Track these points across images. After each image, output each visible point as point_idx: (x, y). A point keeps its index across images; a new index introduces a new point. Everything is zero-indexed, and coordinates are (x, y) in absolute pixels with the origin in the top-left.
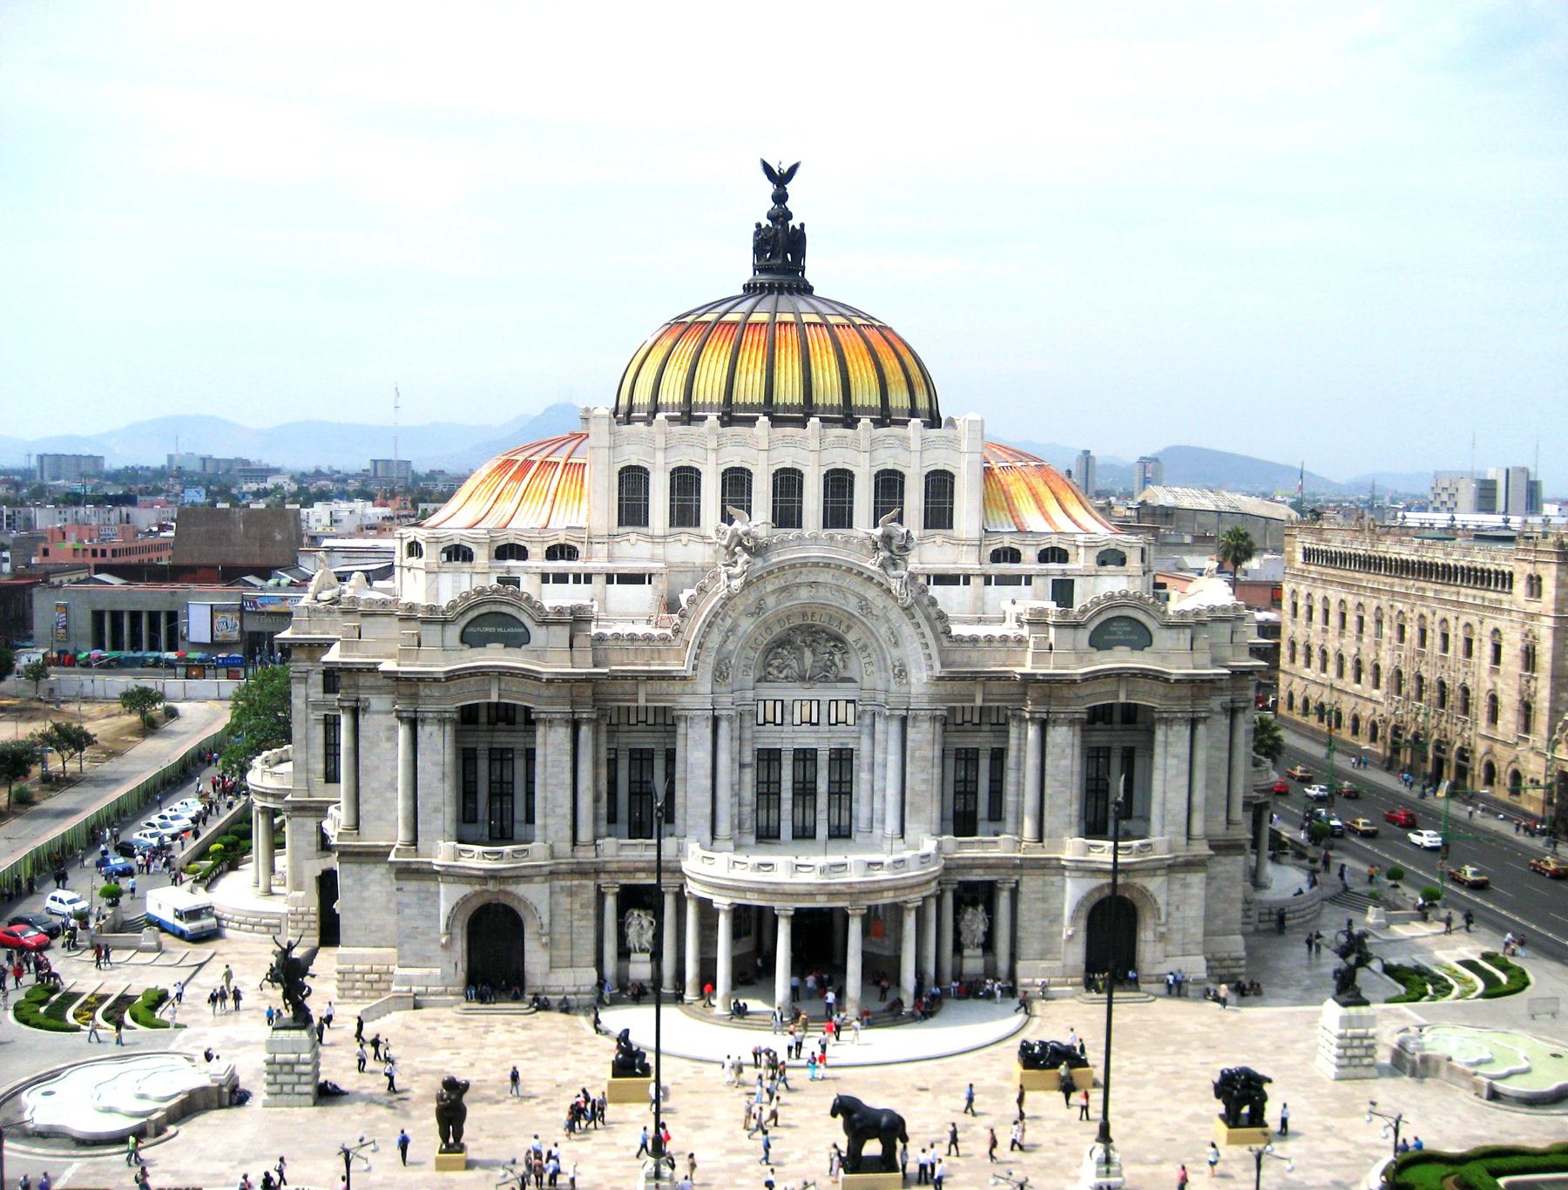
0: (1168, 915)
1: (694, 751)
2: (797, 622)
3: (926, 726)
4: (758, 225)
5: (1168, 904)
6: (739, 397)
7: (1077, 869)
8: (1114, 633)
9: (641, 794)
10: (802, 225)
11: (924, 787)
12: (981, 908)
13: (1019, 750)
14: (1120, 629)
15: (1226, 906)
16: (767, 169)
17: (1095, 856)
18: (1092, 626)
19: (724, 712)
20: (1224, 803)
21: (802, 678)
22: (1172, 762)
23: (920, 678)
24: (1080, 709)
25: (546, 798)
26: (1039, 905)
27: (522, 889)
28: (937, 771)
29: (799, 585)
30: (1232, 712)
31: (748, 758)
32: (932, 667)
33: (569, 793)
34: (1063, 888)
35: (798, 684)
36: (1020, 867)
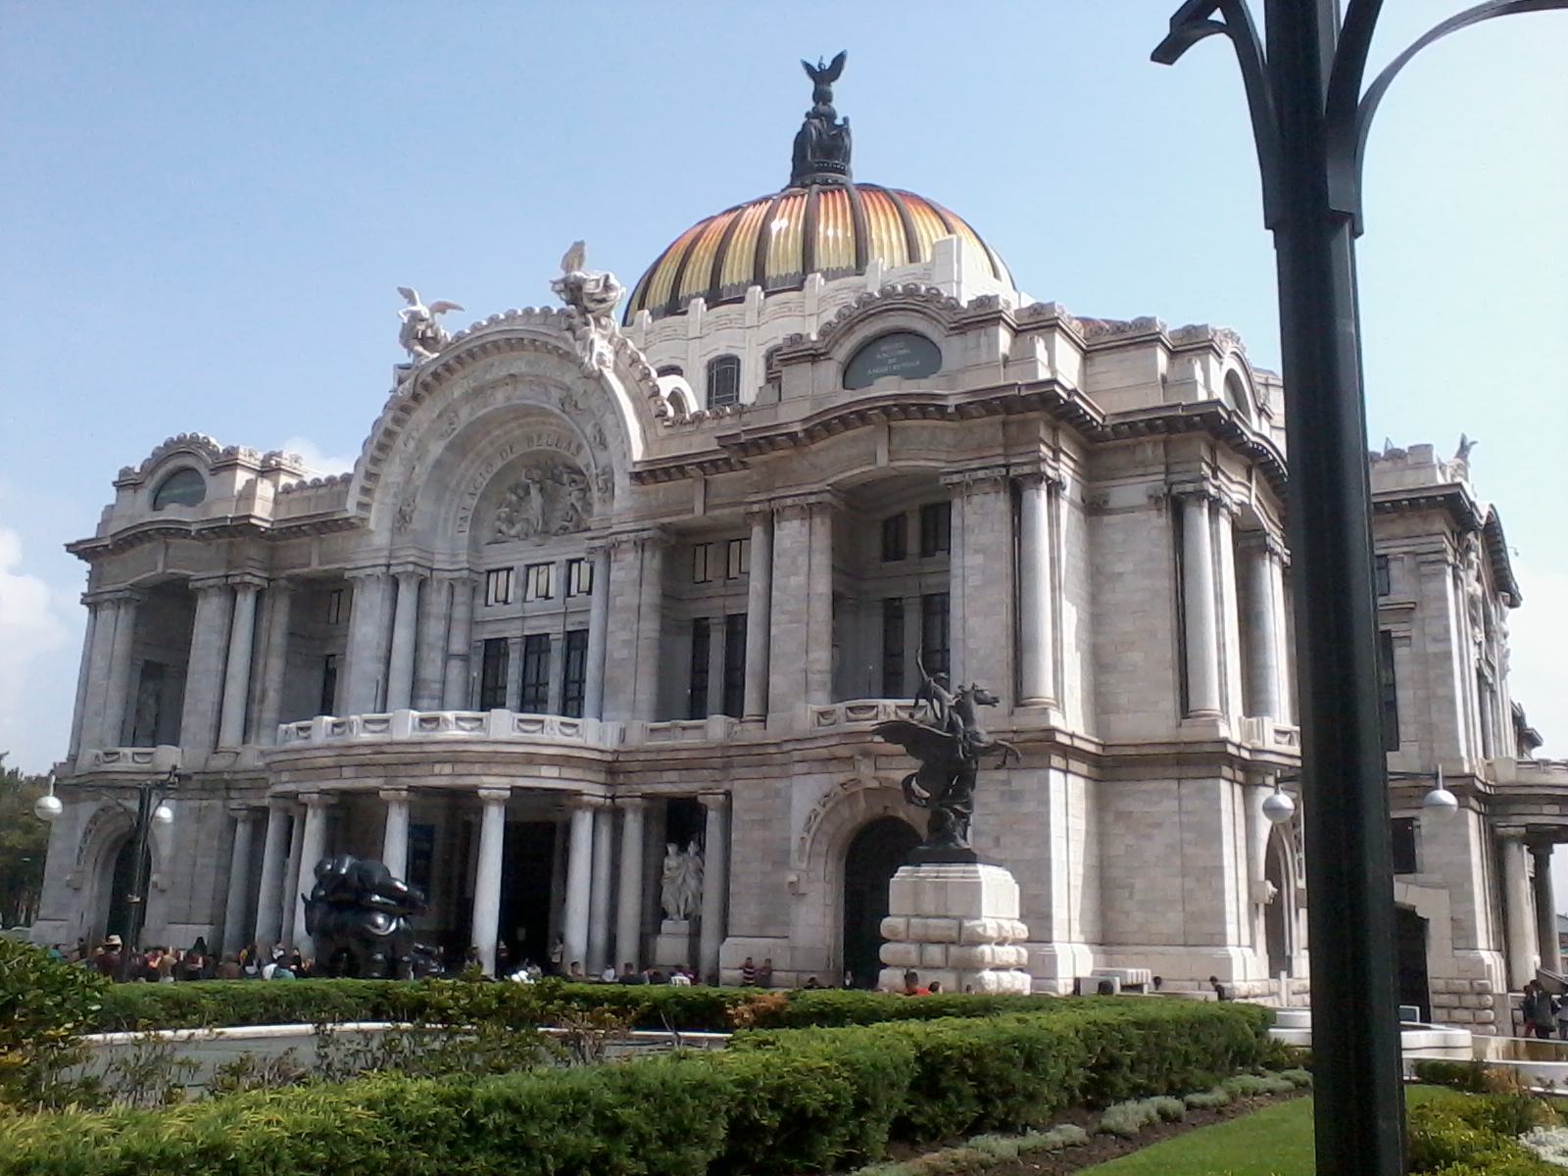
1: (365, 627)
2: (520, 449)
6: (684, 292)
8: (883, 363)
10: (846, 120)
11: (624, 653)
15: (1190, 883)
16: (808, 67)
18: (842, 353)
19: (400, 569)
20: (1170, 676)
22: (974, 560)
23: (622, 482)
26: (757, 834)
29: (495, 385)
30: (1176, 507)
31: (458, 645)
33: (216, 680)
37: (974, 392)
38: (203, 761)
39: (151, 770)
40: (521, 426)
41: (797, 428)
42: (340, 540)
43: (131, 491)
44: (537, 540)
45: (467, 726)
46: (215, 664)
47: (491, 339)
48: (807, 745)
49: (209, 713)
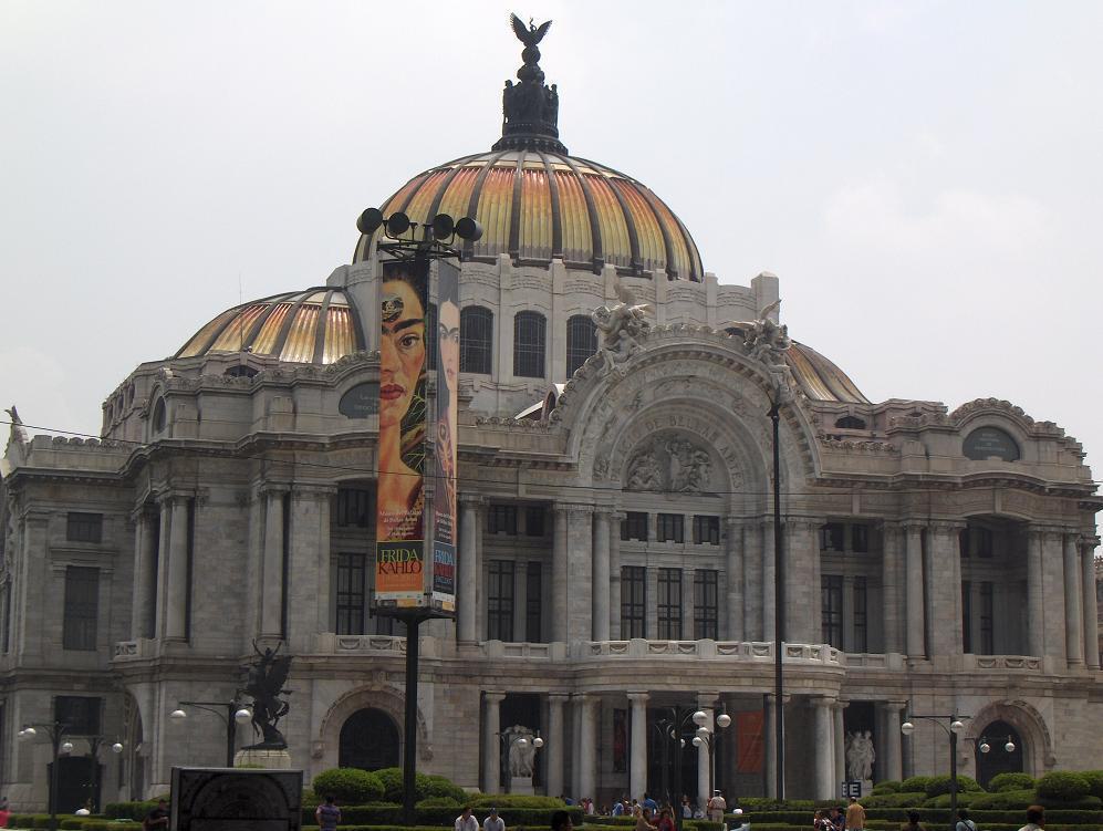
0: (1056, 742)
2: (668, 426)
3: (805, 534)
4: (508, 83)
5: (1056, 733)
6: (525, 240)
10: (554, 87)
11: (805, 601)
12: (868, 734)
13: (896, 565)
14: (990, 438)
16: (518, 25)
18: (966, 432)
19: (605, 510)
21: (667, 491)
22: (1048, 578)
24: (959, 517)
28: (818, 584)
31: (617, 573)
32: (811, 470)
35: (662, 496)
37: (1060, 484)
38: (454, 652)
40: (673, 409)
41: (959, 481)
42: (545, 477)
43: (319, 392)
44: (673, 496)
47: (695, 349)
48: (979, 679)
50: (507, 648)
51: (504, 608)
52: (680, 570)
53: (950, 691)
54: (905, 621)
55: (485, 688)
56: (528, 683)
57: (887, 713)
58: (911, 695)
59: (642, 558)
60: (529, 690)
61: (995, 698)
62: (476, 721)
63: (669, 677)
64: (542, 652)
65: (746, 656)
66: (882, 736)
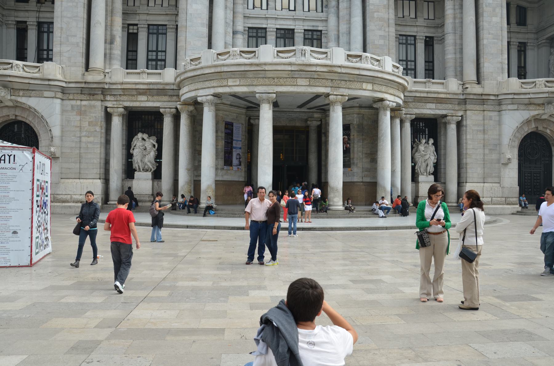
7: (513, 102)
9: (157, 60)
11: (381, 42)
12: (431, 141)
13: (455, 18)
17: (528, 89)
25: (62, 29)
26: (480, 136)
27: (32, 102)
31: (240, 27)
33: (83, 25)
34: (500, 123)
36: (464, 102)
39: (42, 77)
45: (376, 63)
46: (82, 13)
48: (522, 96)
49: (81, 45)
50: (128, 73)
51: (159, 58)
52: (294, 29)
53: (497, 108)
54: (462, 58)
55: (109, 104)
56: (143, 99)
57: (445, 124)
58: (466, 110)
59: (264, 21)
60: (143, 104)
61: (534, 112)
62: (99, 129)
63: (230, 80)
64: (157, 76)
65: (303, 58)
66: (442, 143)
